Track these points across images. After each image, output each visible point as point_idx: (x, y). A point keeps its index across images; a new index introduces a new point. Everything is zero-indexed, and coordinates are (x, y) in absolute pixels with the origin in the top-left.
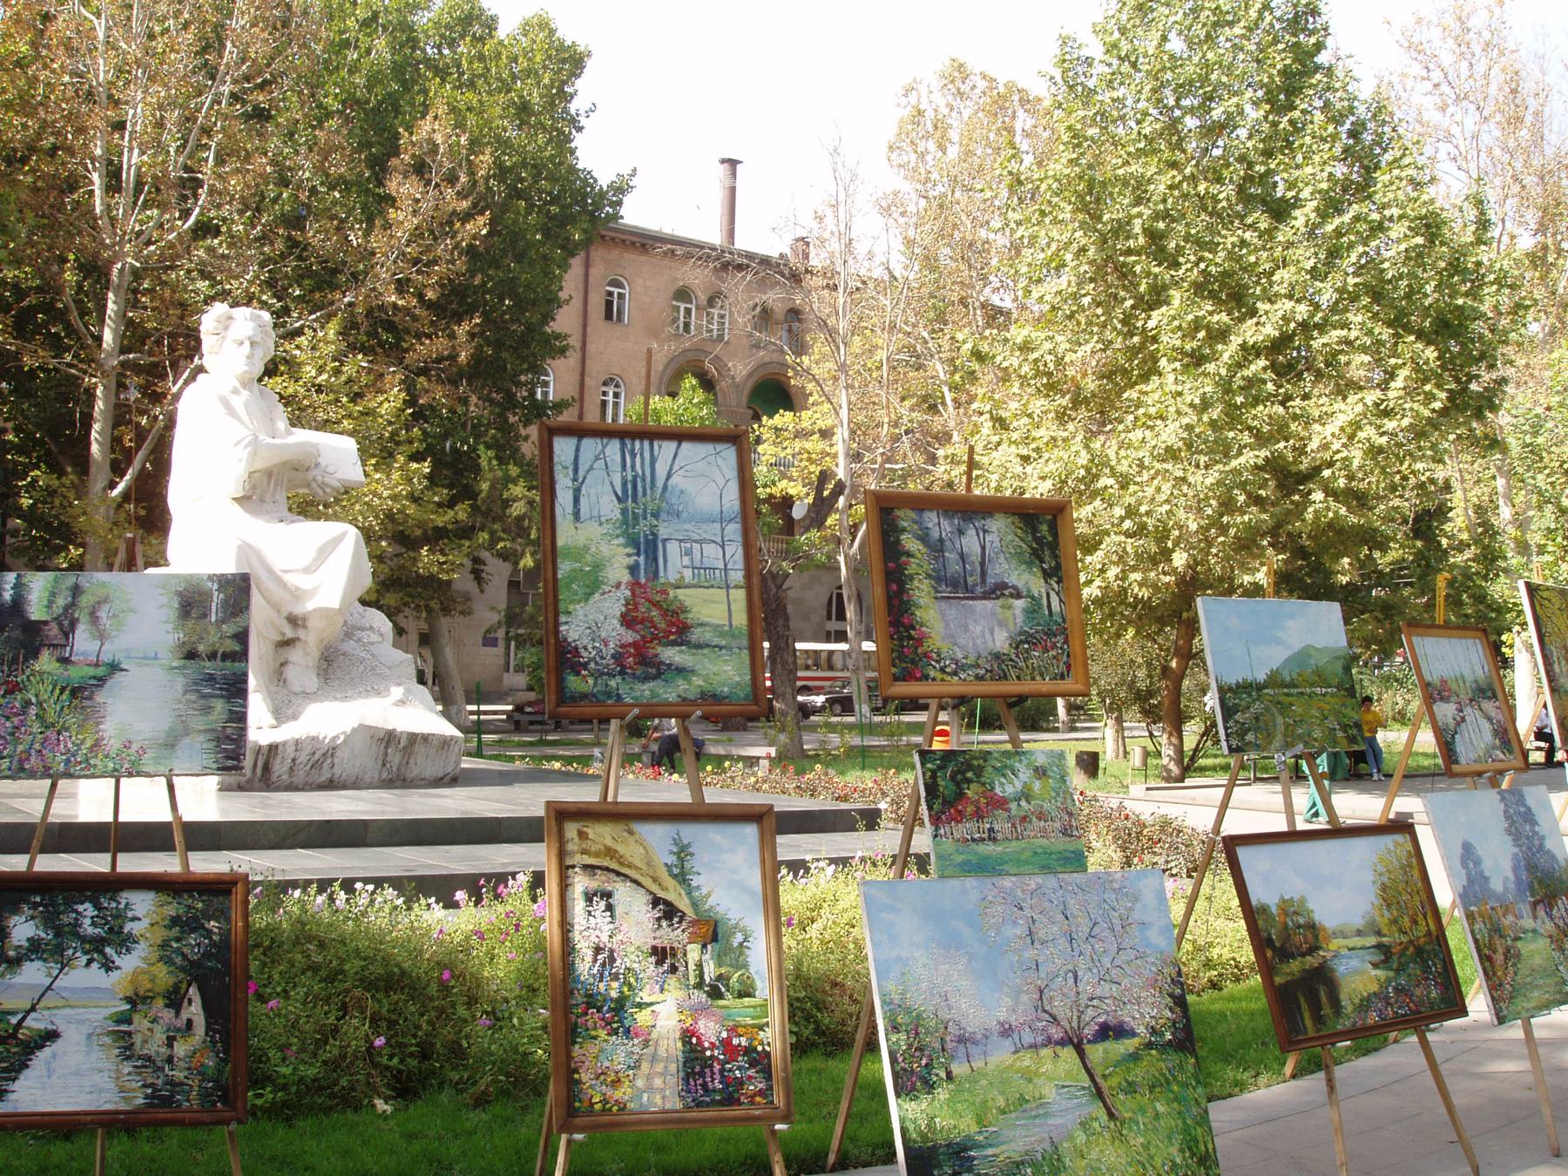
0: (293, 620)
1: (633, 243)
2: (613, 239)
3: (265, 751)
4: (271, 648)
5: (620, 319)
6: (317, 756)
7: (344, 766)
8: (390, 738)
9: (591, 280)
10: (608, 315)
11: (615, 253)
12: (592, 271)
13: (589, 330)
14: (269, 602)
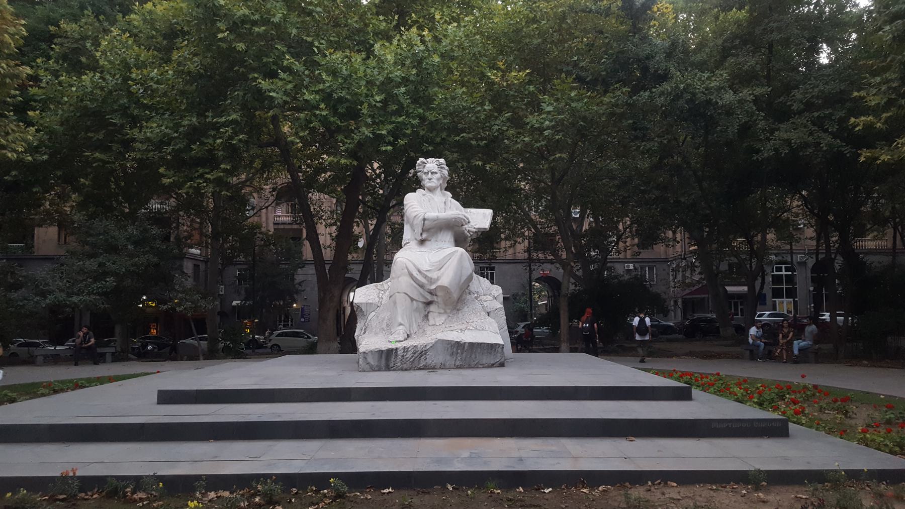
0: (431, 292)
4: (421, 306)
7: (431, 359)
8: (458, 345)
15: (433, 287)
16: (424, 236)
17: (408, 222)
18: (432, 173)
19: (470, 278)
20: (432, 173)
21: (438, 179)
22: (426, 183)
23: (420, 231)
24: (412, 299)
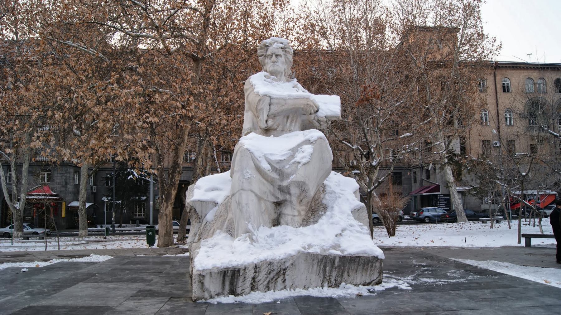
0: (281, 189)
1: (509, 67)
2: (502, 67)
3: (229, 274)
4: (271, 207)
5: (508, 91)
6: (271, 276)
9: (497, 81)
10: (504, 91)
11: (504, 71)
12: (497, 78)
13: (498, 96)
14: (267, 181)
15: (285, 183)
16: (270, 123)
17: (250, 109)
18: (277, 56)
19: (327, 175)
20: (277, 56)
21: (283, 63)
22: (269, 66)
23: (265, 117)
24: (260, 199)
